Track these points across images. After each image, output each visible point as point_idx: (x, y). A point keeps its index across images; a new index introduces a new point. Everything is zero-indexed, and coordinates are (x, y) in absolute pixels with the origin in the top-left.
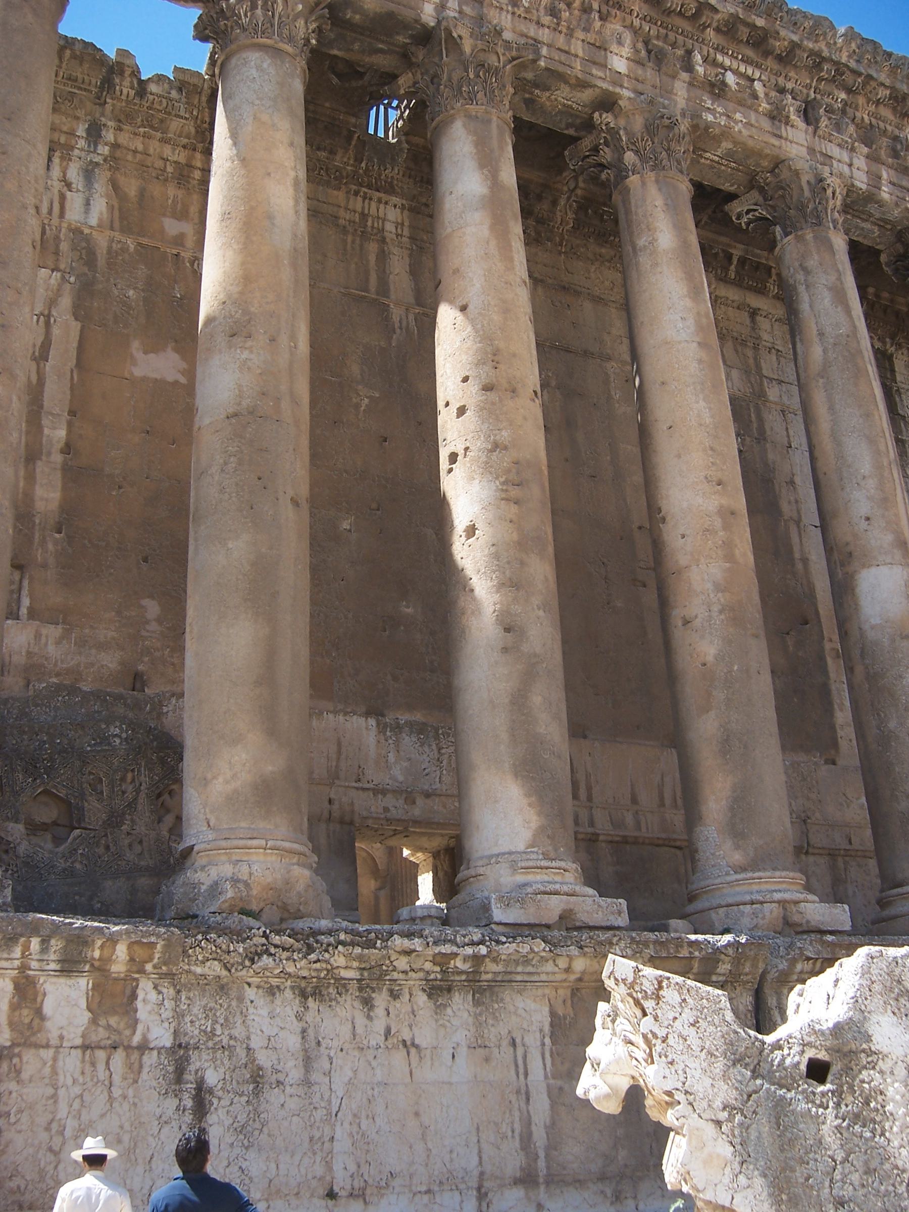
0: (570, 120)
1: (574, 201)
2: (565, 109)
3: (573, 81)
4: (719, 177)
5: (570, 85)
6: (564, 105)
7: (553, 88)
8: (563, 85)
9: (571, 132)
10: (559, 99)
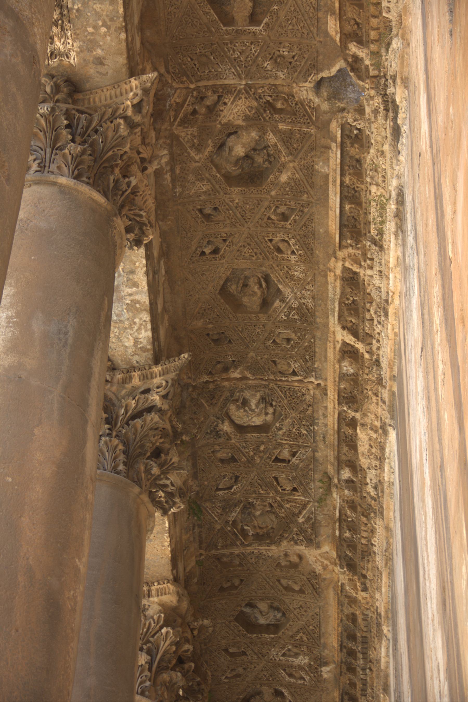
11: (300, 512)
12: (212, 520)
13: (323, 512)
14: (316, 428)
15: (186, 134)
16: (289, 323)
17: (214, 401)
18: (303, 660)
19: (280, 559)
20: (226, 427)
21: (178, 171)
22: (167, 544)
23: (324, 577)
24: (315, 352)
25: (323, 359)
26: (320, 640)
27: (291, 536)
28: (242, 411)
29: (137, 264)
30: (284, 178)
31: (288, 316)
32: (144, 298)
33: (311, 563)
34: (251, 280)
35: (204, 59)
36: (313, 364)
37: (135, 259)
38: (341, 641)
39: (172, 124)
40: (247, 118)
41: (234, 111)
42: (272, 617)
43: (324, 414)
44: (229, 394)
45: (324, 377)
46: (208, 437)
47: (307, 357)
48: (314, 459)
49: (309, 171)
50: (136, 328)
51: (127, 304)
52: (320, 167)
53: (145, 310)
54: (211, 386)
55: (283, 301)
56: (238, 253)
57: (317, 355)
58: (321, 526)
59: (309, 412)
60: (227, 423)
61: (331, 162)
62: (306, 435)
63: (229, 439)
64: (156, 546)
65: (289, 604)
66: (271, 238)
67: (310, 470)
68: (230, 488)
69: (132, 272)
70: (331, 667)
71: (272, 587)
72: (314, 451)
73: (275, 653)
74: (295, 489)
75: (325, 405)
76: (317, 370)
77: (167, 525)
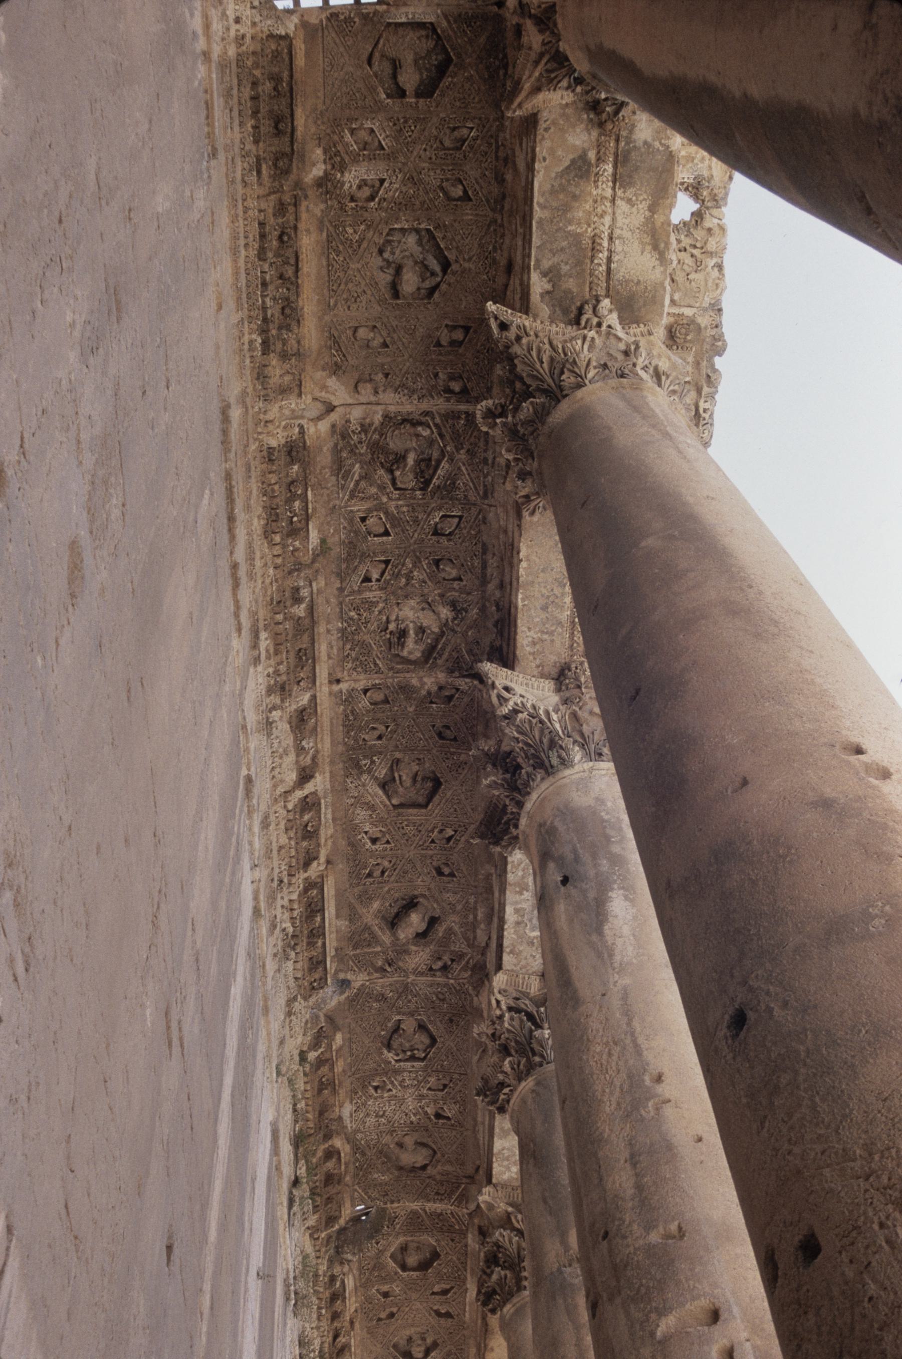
0: (565, 268)
1: (301, 427)
2: (586, 242)
3: (659, 219)
4: (545, 608)
5: (649, 221)
6: (595, 239)
7: (630, 193)
8: (643, 206)
9: (538, 284)
10: (607, 220)
11: (357, 483)
12: (469, 468)
13: (328, 492)
14: (340, 624)
15: (459, 946)
16: (371, 753)
17: (455, 655)
18: (351, 178)
19: (384, 386)
20: (445, 612)
21: (471, 917)
22: (524, 564)
23: (324, 374)
24: (343, 726)
25: (334, 721)
26: (328, 236)
27: (369, 436)
28: (424, 625)
29: (512, 931)
30: (376, 905)
31: (373, 762)
32: (510, 896)
33: (343, 388)
34: (408, 785)
35: (441, 996)
36: (345, 711)
37: (513, 936)
38: (297, 277)
39: (471, 957)
40: (407, 952)
41: (419, 957)
42: (397, 252)
43: (332, 647)
44: (438, 661)
45: (333, 698)
46: (465, 606)
47: (351, 718)
48: (341, 576)
49: (353, 916)
50: (522, 865)
51: (527, 891)
52: (343, 924)
53: (511, 885)
54: (457, 674)
55: (376, 778)
56: (420, 828)
57: (341, 723)
58: (331, 467)
59: (348, 647)
60: (443, 616)
61: (334, 936)
62: (350, 610)
63: (442, 596)
64: (537, 560)
65: (373, 299)
66: (388, 846)
67: (346, 560)
68: (443, 516)
69: (518, 923)
70: (311, 176)
71: (394, 330)
72: (341, 590)
73: (394, 188)
74: (363, 519)
75: (330, 661)
76: (340, 702)
77: (520, 596)
